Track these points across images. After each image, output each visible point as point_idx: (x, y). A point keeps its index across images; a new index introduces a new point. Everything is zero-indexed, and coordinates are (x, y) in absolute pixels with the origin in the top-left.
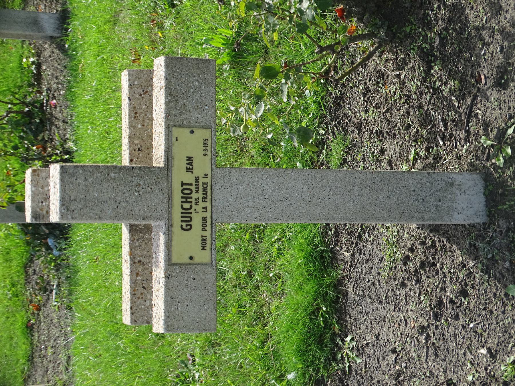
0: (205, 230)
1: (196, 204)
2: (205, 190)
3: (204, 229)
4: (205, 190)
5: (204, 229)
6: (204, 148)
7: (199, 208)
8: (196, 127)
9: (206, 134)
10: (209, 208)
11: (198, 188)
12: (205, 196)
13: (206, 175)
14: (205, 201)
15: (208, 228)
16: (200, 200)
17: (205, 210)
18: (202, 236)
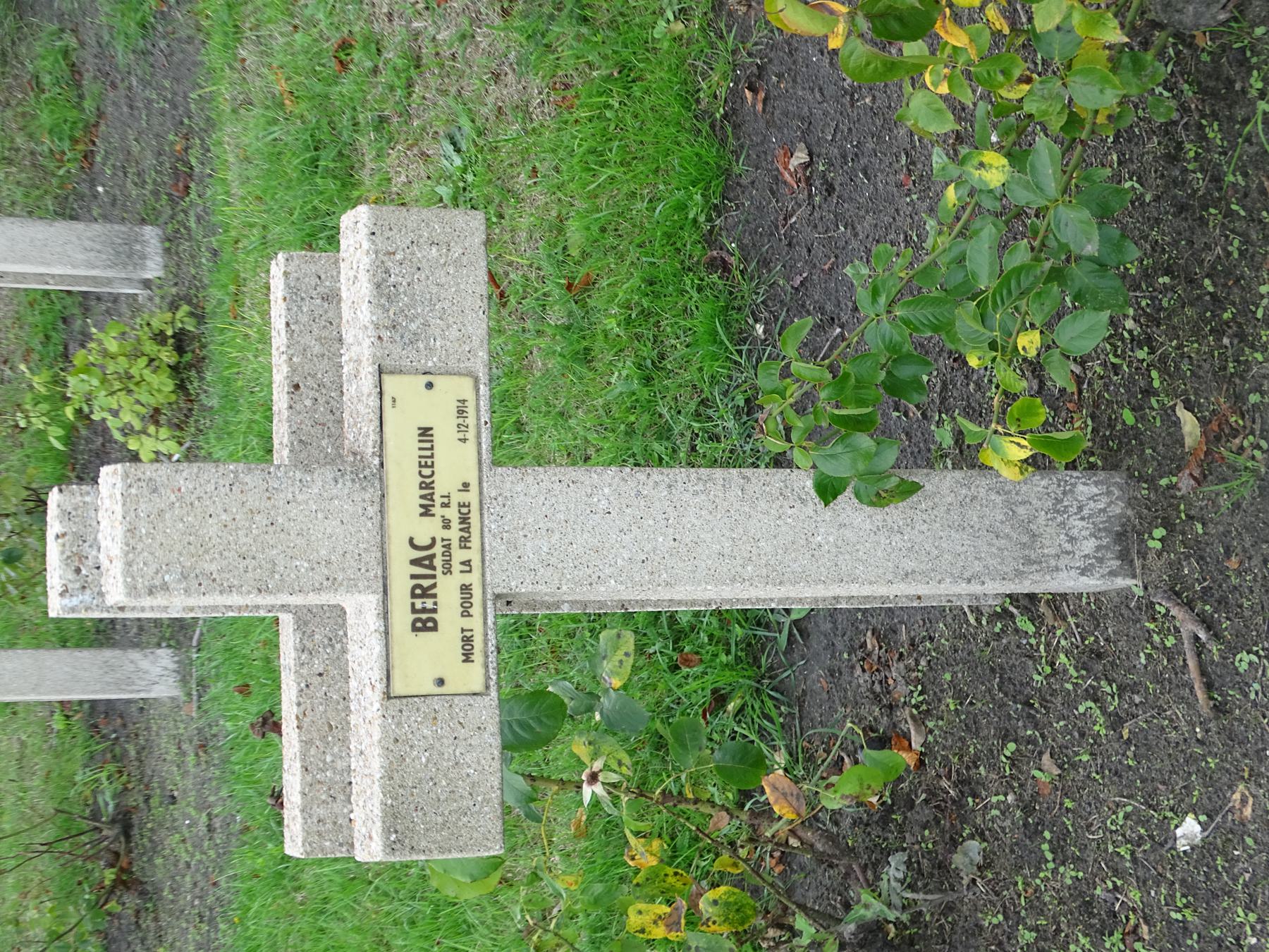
0: (470, 615)
2: (464, 519)
3: (466, 613)
4: (464, 519)
5: (466, 613)
9: (464, 387)
10: (476, 563)
12: (466, 535)
13: (466, 486)
14: (465, 547)
16: (455, 544)
18: (463, 630)
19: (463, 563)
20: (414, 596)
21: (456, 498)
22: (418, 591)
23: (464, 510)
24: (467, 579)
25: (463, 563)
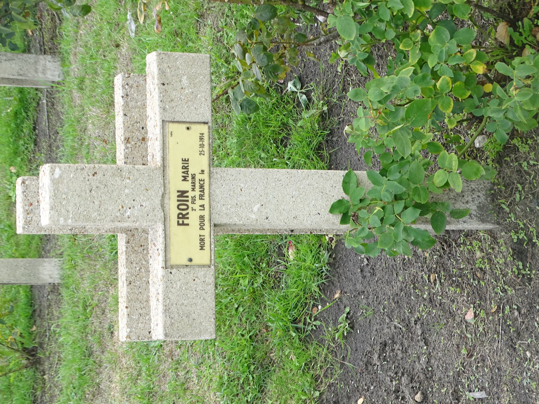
0: (203, 229)
1: (193, 203)
2: (202, 187)
3: (202, 228)
4: (202, 187)
5: (202, 228)
6: (201, 143)
7: (196, 206)
8: (190, 123)
10: (207, 207)
11: (194, 186)
12: (202, 194)
13: (203, 171)
14: (202, 199)
15: (207, 226)
17: (203, 208)
18: (200, 236)
19: (200, 206)
20: (179, 218)
21: (198, 177)
22: (181, 216)
23: (202, 183)
24: (202, 213)
25: (200, 206)
